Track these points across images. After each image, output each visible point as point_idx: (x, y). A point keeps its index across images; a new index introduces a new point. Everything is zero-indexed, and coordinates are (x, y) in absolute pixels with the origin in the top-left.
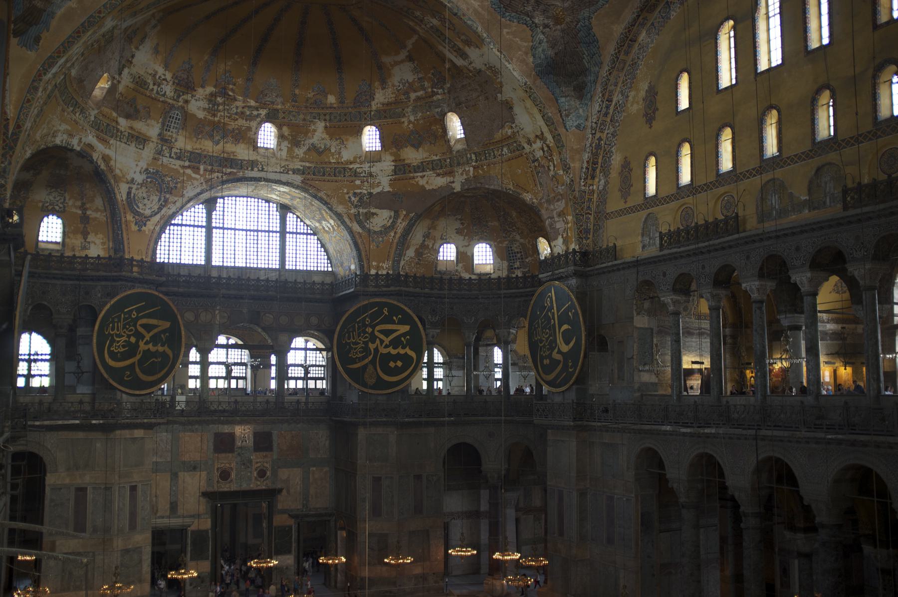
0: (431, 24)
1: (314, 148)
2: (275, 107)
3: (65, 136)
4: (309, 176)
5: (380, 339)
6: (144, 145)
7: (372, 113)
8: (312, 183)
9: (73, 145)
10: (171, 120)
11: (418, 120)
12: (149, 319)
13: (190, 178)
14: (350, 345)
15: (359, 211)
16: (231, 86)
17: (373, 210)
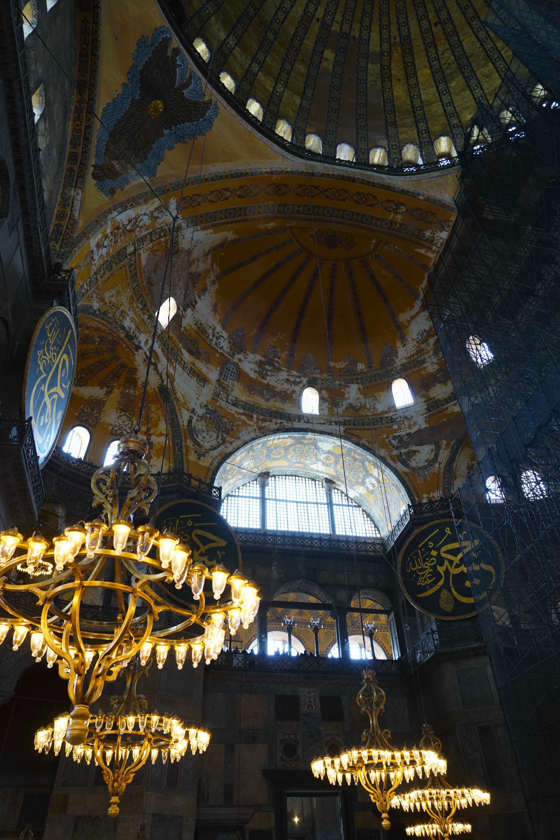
0: (441, 241)
1: (351, 407)
2: (314, 376)
3: (133, 325)
4: (350, 427)
5: (448, 560)
6: (204, 384)
7: (398, 368)
8: (354, 432)
9: (140, 342)
10: (228, 371)
11: (440, 359)
12: (205, 532)
13: (244, 423)
14: (417, 574)
15: (401, 453)
16: (277, 359)
17: (414, 448)
